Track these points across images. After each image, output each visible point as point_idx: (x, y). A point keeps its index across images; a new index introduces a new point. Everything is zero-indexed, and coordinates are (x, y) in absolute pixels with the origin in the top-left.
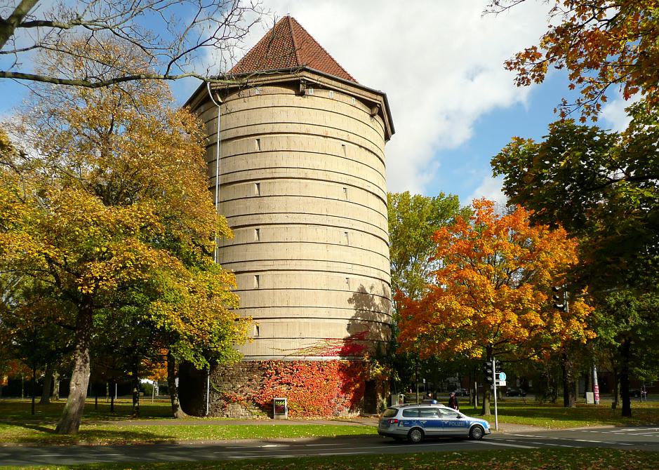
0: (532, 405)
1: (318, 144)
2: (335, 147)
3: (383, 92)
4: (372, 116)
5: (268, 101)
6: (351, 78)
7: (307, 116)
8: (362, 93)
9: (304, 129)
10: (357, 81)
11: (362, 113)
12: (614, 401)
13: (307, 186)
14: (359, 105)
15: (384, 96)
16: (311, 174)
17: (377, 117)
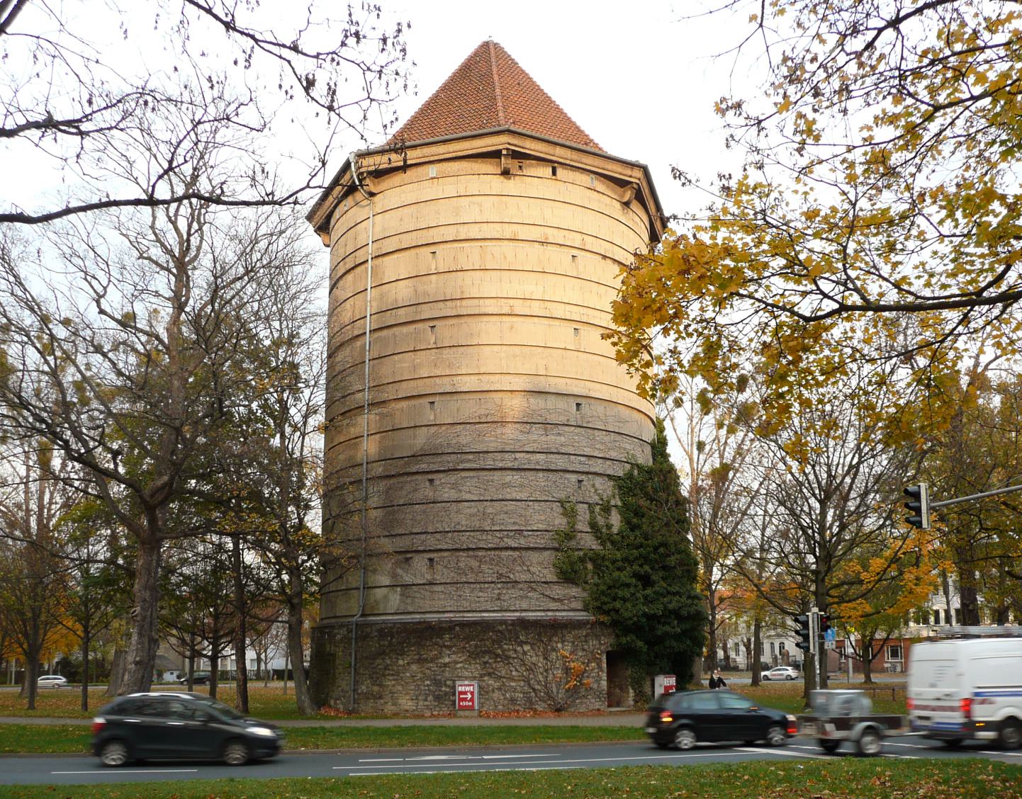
0: (331, 731)
1: (530, 256)
2: (562, 260)
3: (642, 162)
4: (626, 204)
5: (448, 188)
6: (592, 141)
7: (514, 210)
8: (606, 167)
9: (508, 231)
10: (601, 146)
11: (608, 201)
12: (742, 666)
13: (512, 328)
14: (600, 186)
15: (645, 170)
16: (519, 308)
17: (635, 206)
